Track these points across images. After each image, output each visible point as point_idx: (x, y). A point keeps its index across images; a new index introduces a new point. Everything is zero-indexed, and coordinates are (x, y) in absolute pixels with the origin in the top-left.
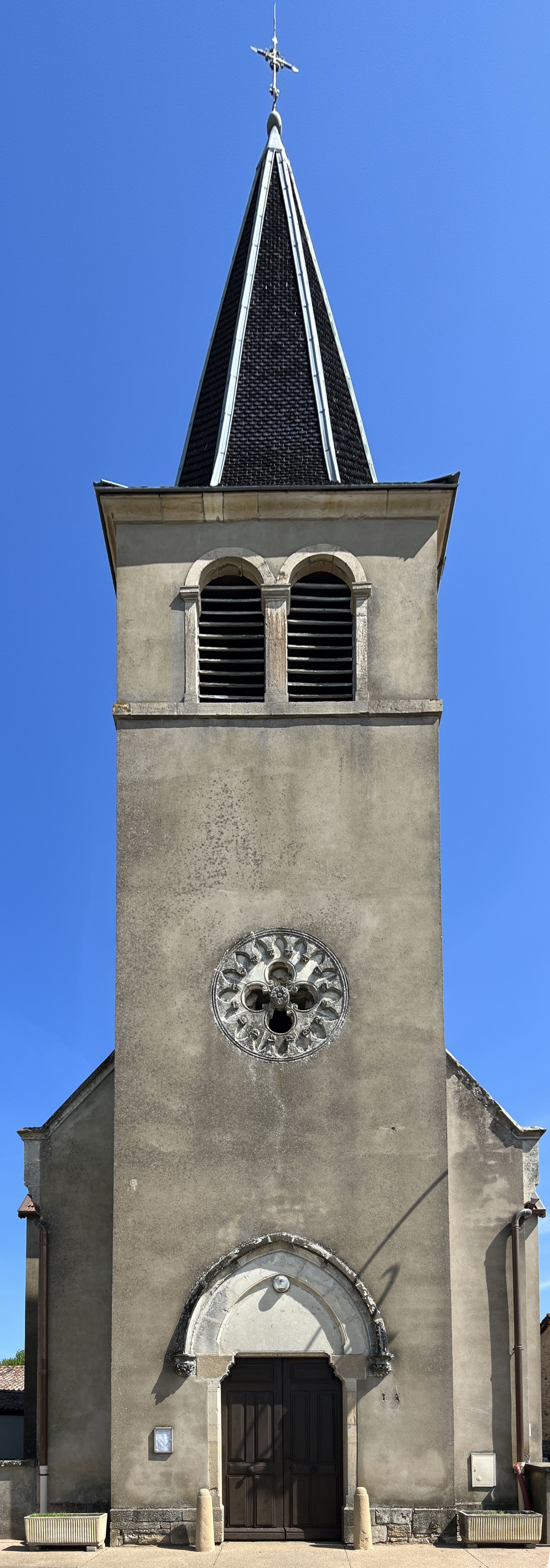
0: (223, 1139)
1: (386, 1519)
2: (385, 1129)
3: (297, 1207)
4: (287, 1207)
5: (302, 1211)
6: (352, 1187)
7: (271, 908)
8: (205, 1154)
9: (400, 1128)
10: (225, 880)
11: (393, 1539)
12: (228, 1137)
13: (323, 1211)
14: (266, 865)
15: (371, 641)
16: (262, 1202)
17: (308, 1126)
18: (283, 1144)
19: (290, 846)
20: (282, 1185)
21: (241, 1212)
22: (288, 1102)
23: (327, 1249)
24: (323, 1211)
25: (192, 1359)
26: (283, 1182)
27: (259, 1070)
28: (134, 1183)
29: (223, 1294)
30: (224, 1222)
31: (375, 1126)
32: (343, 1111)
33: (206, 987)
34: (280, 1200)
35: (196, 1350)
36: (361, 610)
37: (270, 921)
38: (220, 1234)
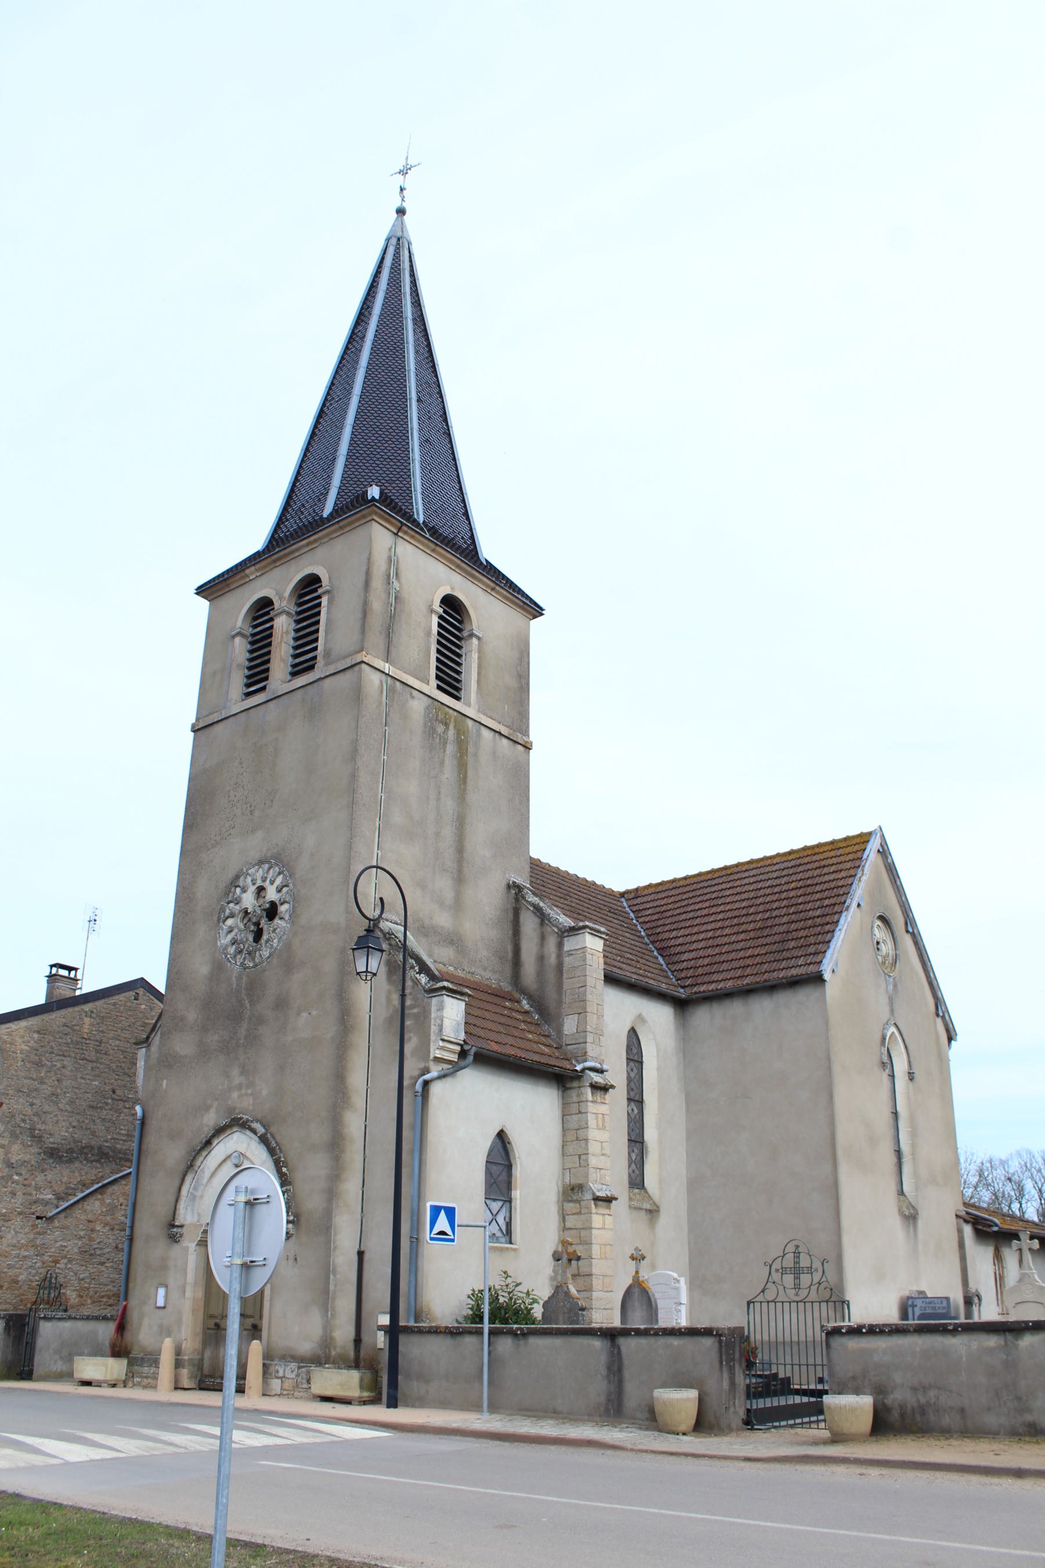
0: (213, 1039)
1: (281, 1374)
2: (305, 1015)
3: (249, 1091)
4: (243, 1091)
5: (251, 1094)
6: (281, 1068)
7: (255, 845)
8: (204, 1053)
9: (314, 1013)
10: (233, 832)
11: (285, 1392)
12: (216, 1037)
13: (264, 1093)
14: (257, 813)
15: (329, 620)
16: (230, 1089)
17: (260, 1020)
18: (246, 1037)
19: (270, 794)
20: (242, 1073)
21: (217, 1100)
22: (252, 1003)
23: (264, 1126)
24: (264, 1093)
25: (182, 1226)
26: (242, 1073)
27: (239, 978)
28: (165, 1082)
29: (203, 1171)
30: (208, 1108)
31: (299, 1014)
32: (282, 1004)
33: (215, 918)
34: (240, 1087)
35: (185, 1219)
36: (324, 600)
37: (255, 855)
38: (205, 1120)
